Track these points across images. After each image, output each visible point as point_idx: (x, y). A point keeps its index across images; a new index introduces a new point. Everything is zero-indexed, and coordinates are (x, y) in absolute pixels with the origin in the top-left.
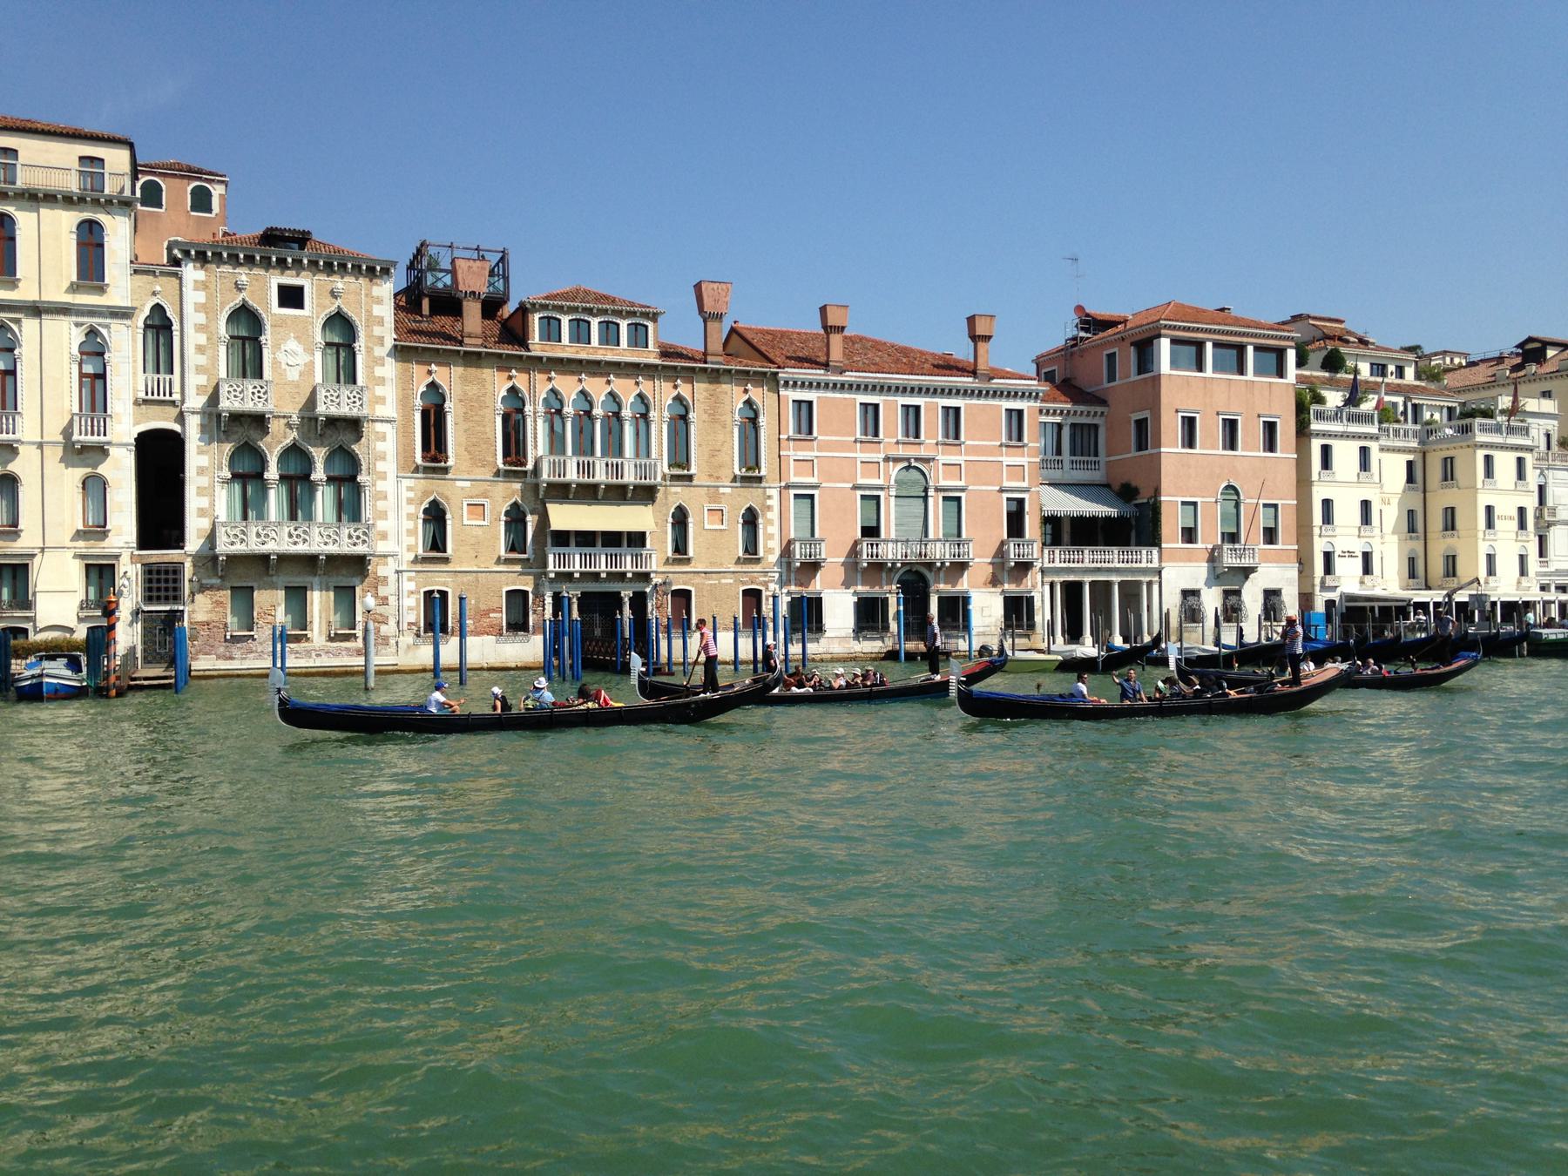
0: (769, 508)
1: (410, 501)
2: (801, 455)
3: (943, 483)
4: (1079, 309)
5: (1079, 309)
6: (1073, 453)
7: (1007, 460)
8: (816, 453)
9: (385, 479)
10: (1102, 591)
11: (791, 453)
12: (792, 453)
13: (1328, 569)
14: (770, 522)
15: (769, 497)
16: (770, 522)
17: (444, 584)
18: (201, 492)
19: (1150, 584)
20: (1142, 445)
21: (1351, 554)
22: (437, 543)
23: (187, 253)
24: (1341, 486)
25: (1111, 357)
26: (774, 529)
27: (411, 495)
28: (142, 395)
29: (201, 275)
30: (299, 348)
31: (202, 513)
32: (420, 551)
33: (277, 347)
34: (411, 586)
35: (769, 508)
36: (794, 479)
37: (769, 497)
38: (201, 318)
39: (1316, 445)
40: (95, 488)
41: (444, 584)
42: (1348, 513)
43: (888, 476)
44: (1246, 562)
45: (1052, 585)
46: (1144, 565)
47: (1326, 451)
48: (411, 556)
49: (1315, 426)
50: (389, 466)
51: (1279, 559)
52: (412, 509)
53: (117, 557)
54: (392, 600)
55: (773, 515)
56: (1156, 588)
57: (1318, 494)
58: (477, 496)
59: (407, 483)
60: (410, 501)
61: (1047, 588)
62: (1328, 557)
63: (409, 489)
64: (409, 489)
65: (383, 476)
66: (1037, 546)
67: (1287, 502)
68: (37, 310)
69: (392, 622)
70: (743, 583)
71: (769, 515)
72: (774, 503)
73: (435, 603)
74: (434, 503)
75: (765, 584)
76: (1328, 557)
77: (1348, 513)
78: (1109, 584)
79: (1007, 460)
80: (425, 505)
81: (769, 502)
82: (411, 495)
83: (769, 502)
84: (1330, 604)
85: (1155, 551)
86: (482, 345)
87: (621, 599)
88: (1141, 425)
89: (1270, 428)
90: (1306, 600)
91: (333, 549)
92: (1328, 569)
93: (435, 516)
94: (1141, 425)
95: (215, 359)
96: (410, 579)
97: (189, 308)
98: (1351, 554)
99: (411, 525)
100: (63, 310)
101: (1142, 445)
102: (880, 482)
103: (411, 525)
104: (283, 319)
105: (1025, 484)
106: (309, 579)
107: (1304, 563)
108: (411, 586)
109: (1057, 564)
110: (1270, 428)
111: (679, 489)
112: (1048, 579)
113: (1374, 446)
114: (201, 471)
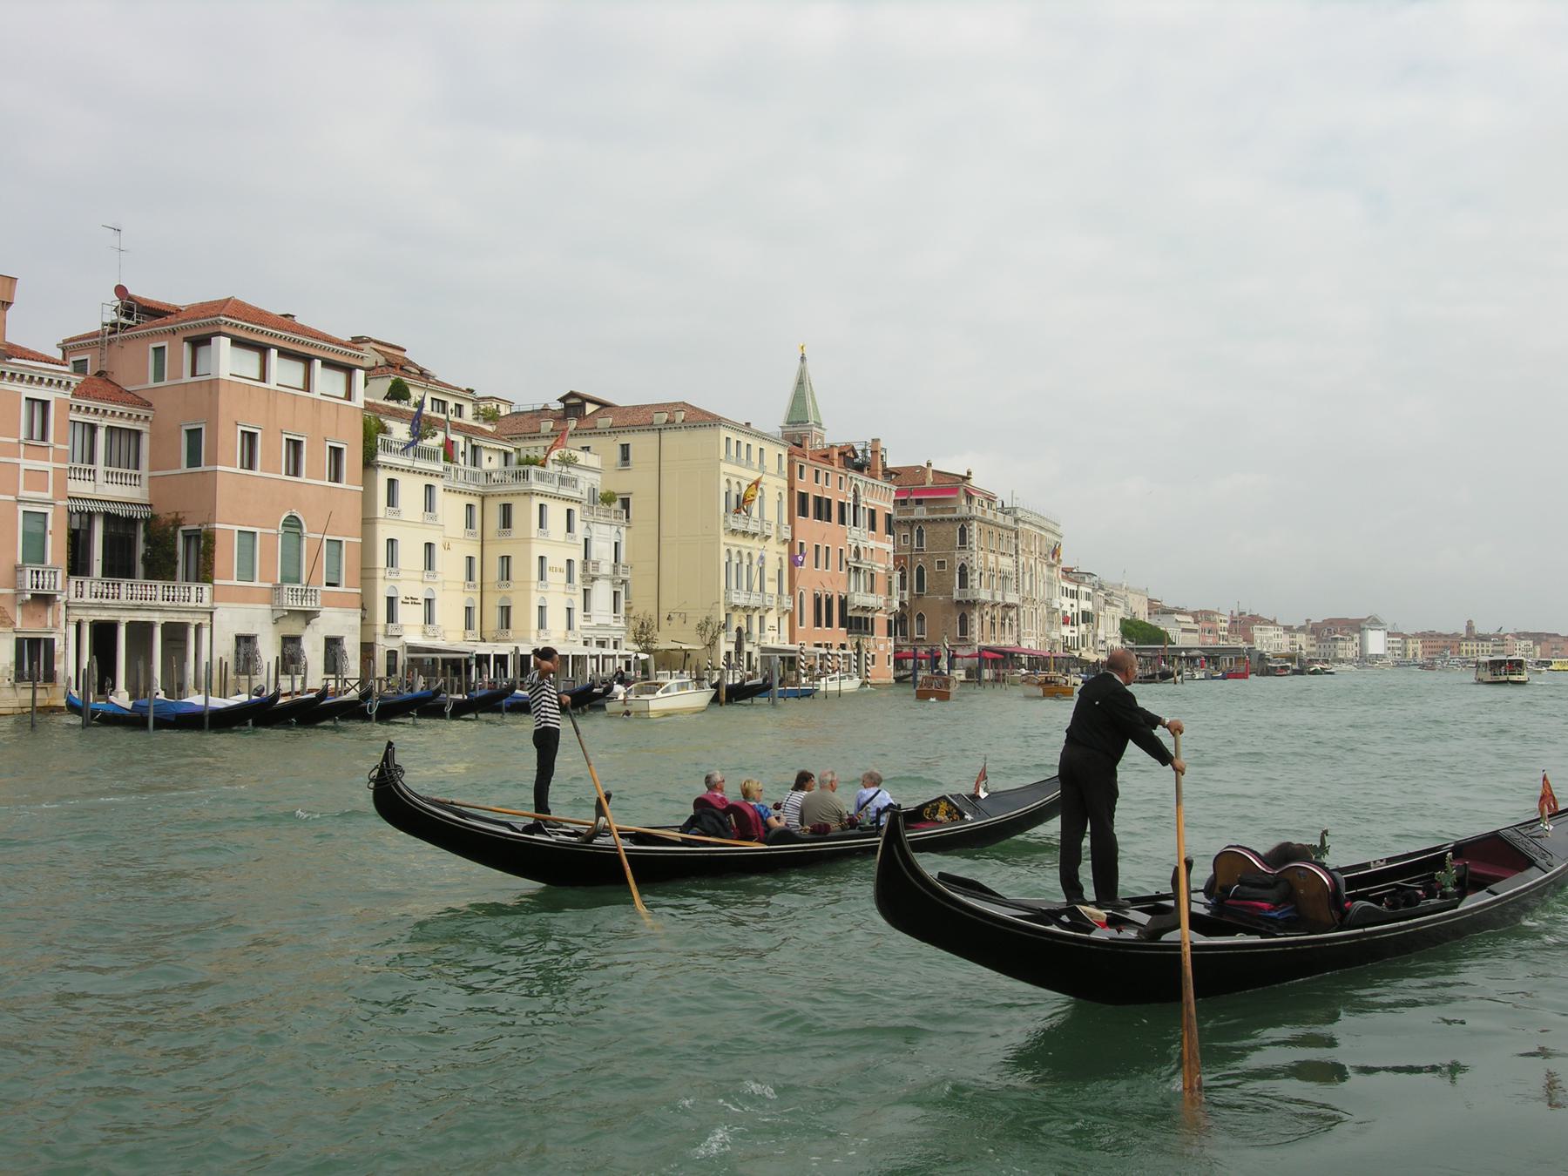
4: (121, 291)
5: (121, 291)
6: (109, 463)
7: (25, 464)
10: (141, 632)
13: (391, 617)
19: (198, 627)
20: (194, 459)
21: (414, 601)
24: (404, 525)
25: (159, 351)
39: (382, 477)
42: (410, 555)
44: (308, 605)
45: (79, 625)
46: (193, 603)
47: (392, 483)
49: (382, 457)
51: (341, 602)
56: (206, 632)
57: (383, 533)
61: (73, 629)
62: (391, 601)
66: (62, 574)
67: (352, 539)
76: (391, 601)
77: (410, 555)
78: (149, 626)
79: (25, 464)
84: (392, 654)
85: (207, 588)
88: (194, 435)
89: (337, 453)
90: (367, 649)
92: (391, 617)
94: (194, 435)
98: (414, 601)
101: (194, 459)
105: (49, 495)
107: (366, 608)
109: (87, 599)
110: (337, 453)
112: (74, 619)
113: (439, 484)
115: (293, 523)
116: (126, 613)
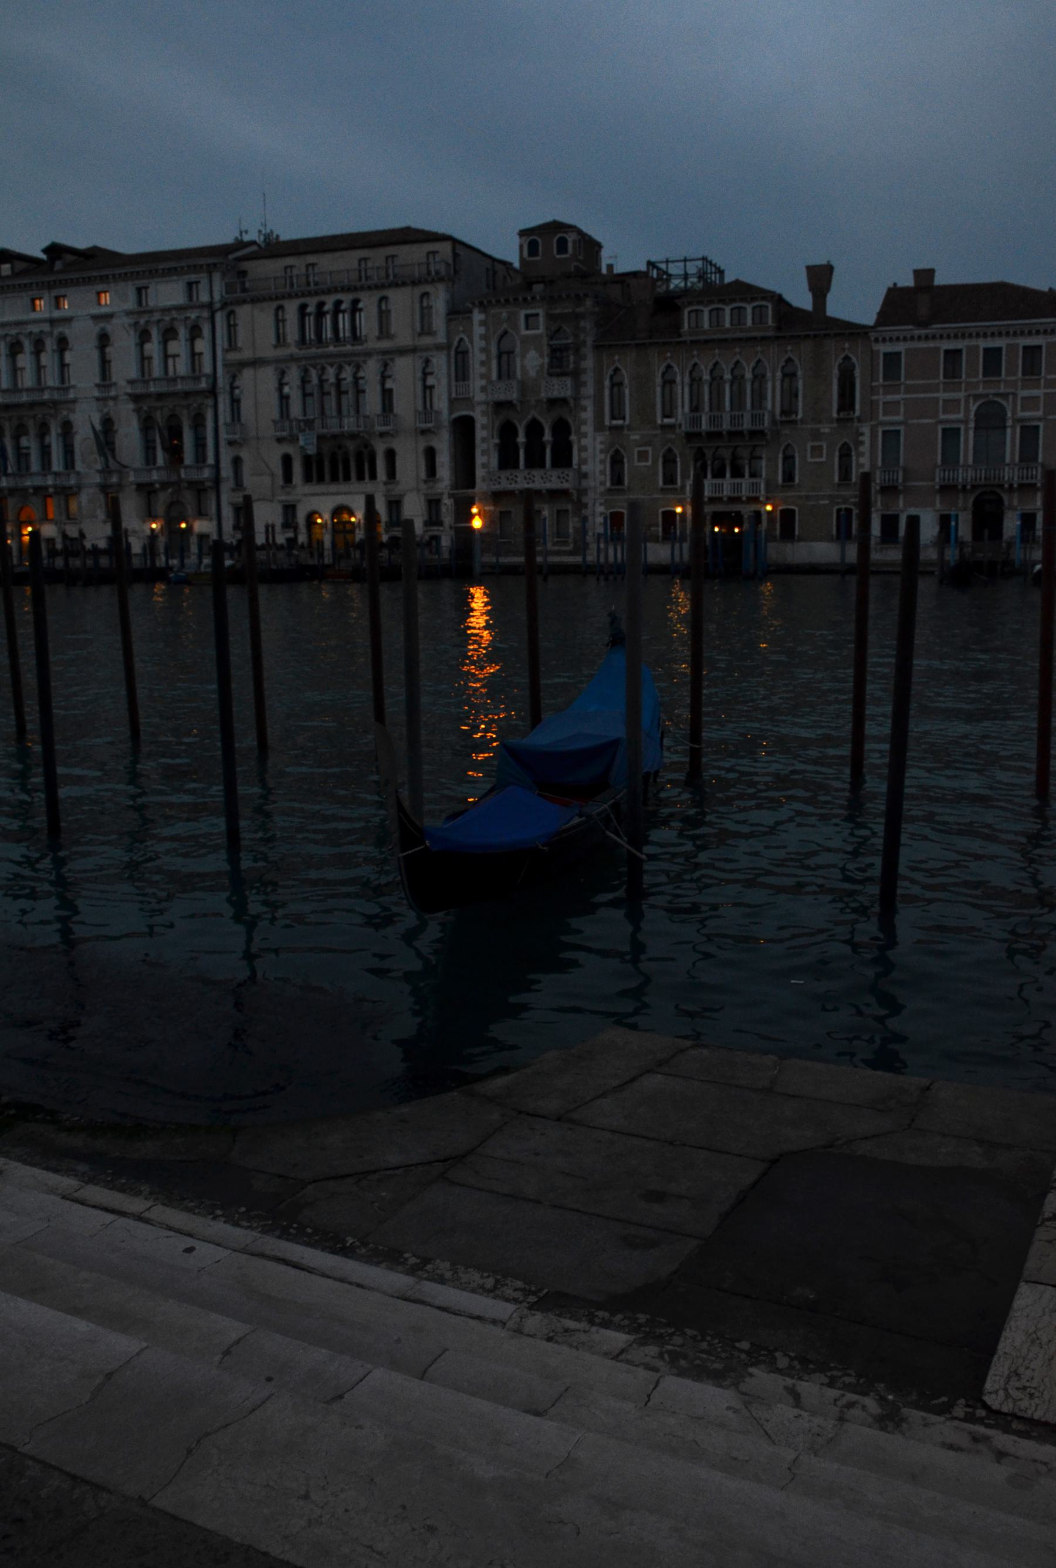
0: (862, 443)
1: (601, 451)
2: (889, 398)
3: (1021, 414)
9: (586, 437)
11: (881, 397)
12: (881, 398)
14: (862, 454)
15: (862, 434)
16: (862, 454)
18: (483, 453)
22: (617, 479)
23: (473, 304)
27: (602, 447)
28: (454, 395)
29: (482, 317)
31: (484, 466)
32: (608, 484)
33: (523, 357)
34: (601, 509)
35: (862, 443)
36: (881, 418)
37: (862, 434)
38: (483, 344)
40: (430, 454)
43: (967, 410)
50: (588, 428)
52: (603, 456)
53: (442, 494)
54: (590, 518)
55: (865, 448)
60: (601, 451)
63: (601, 443)
64: (601, 443)
65: (585, 435)
68: (402, 352)
70: (838, 504)
71: (861, 449)
72: (866, 439)
74: (617, 451)
80: (611, 452)
81: (861, 438)
82: (602, 447)
83: (861, 438)
87: (742, 517)
91: (548, 485)
93: (617, 461)
95: (490, 370)
96: (601, 504)
97: (476, 338)
99: (601, 467)
100: (413, 350)
102: (961, 416)
103: (601, 467)
104: (527, 336)
108: (601, 509)
111: (787, 432)
114: (484, 440)
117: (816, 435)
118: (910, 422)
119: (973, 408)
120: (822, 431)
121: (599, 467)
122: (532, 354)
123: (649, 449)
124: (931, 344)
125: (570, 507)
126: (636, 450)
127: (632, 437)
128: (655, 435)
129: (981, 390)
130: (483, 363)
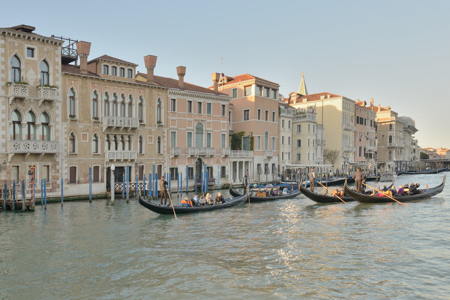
1: (66, 133)
8: (177, 118)
12: (171, 118)
14: (164, 141)
15: (165, 133)
16: (164, 141)
17: (76, 164)
26: (165, 144)
27: (66, 130)
30: (34, 73)
36: (171, 127)
41: (76, 164)
48: (65, 154)
50: (59, 119)
54: (60, 170)
56: (252, 163)
58: (85, 131)
59: (65, 125)
60: (66, 133)
69: (60, 179)
70: (158, 163)
73: (73, 170)
75: (163, 163)
82: (66, 130)
86: (87, 75)
96: (66, 163)
105: (226, 130)
106: (36, 163)
115: (267, 133)
116: (239, 159)
117: (150, 132)
118: (179, 129)
119: (195, 125)
120: (152, 130)
121: (65, 142)
122: (31, 71)
123: (87, 133)
124: (185, 98)
125: (50, 164)
126: (82, 133)
127: (80, 126)
128: (90, 127)
129: (197, 119)
130: (3, 71)
